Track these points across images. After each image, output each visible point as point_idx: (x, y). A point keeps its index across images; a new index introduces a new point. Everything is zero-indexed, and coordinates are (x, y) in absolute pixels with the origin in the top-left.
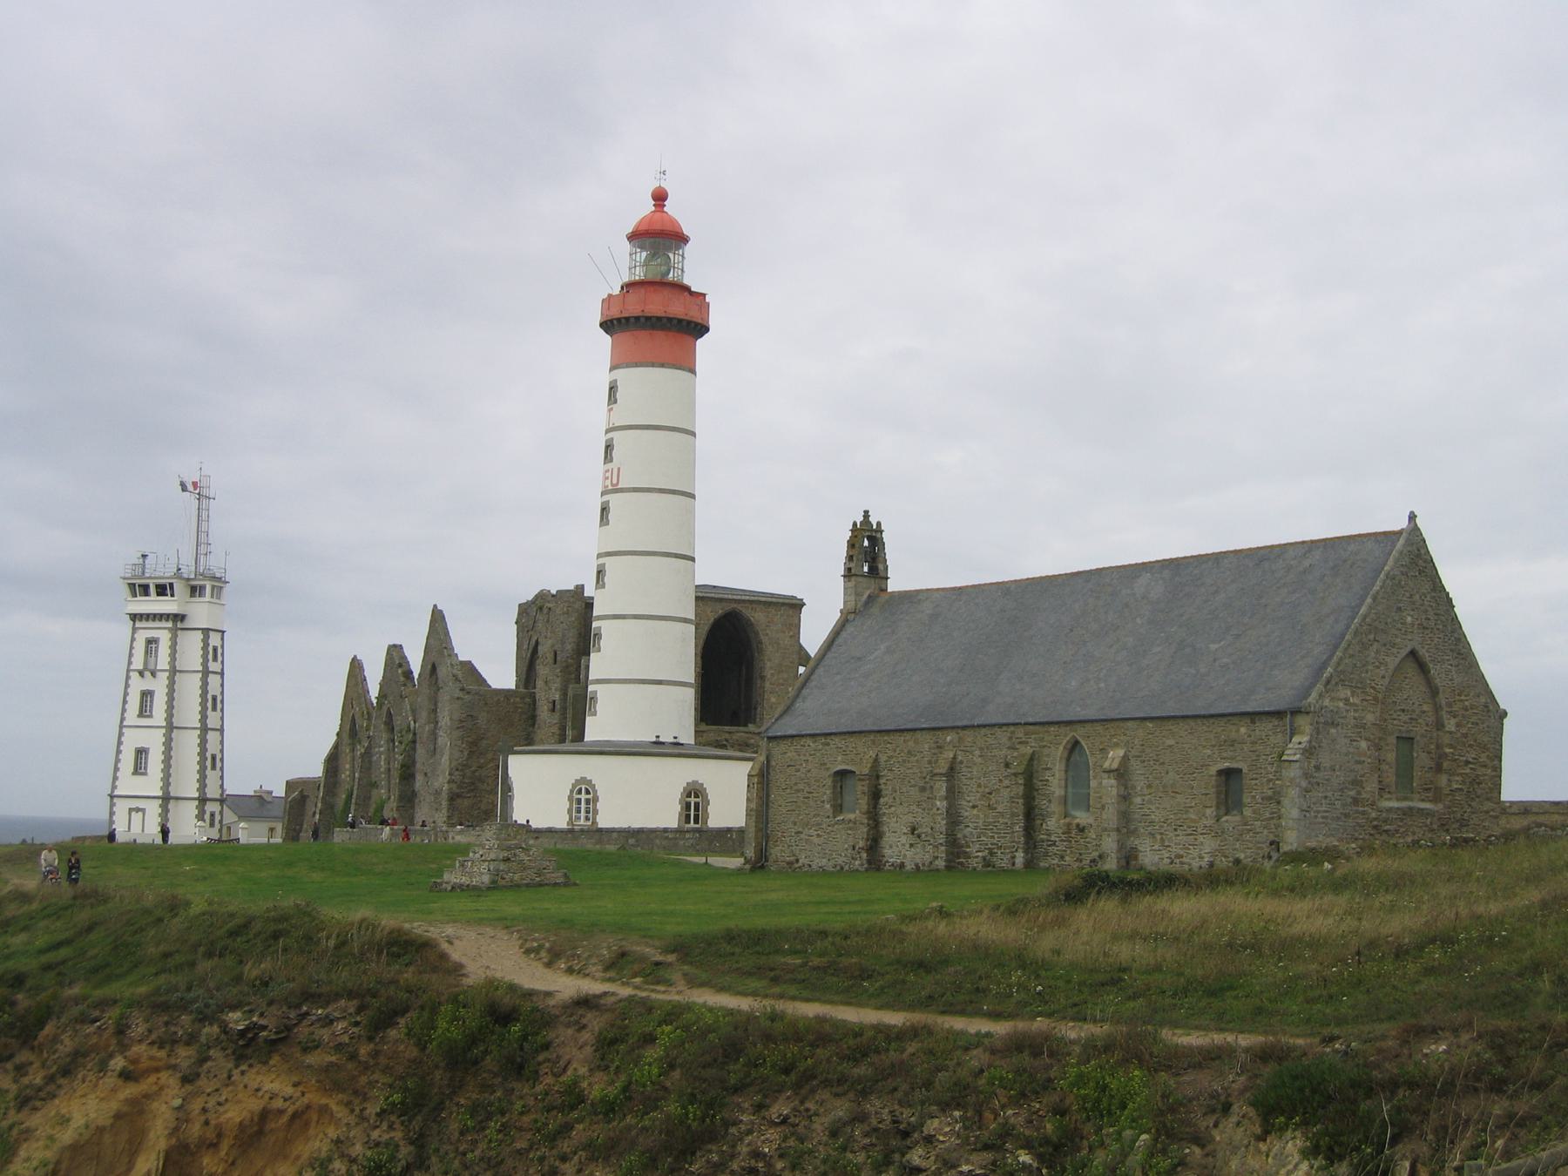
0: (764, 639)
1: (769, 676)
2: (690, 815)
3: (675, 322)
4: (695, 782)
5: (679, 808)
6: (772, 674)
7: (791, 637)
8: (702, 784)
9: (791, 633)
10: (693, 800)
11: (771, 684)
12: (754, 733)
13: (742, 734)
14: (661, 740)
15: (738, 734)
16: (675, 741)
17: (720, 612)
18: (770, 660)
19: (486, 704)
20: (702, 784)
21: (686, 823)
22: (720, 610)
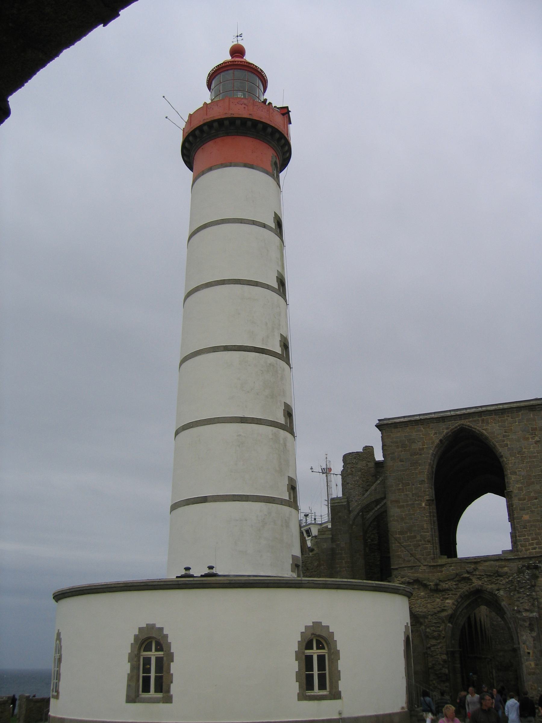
0: (503, 451)
1: (516, 491)
2: (149, 677)
3: (216, 125)
4: (151, 627)
5: (126, 668)
6: (520, 489)
7: (536, 442)
8: (161, 629)
9: (537, 439)
10: (315, 653)
11: (520, 500)
12: (509, 560)
13: (492, 562)
14: (191, 572)
15: (487, 564)
16: (211, 571)
17: (445, 431)
18: (515, 473)
19: (308, 569)
20: (161, 629)
21: (144, 691)
22: (445, 430)
